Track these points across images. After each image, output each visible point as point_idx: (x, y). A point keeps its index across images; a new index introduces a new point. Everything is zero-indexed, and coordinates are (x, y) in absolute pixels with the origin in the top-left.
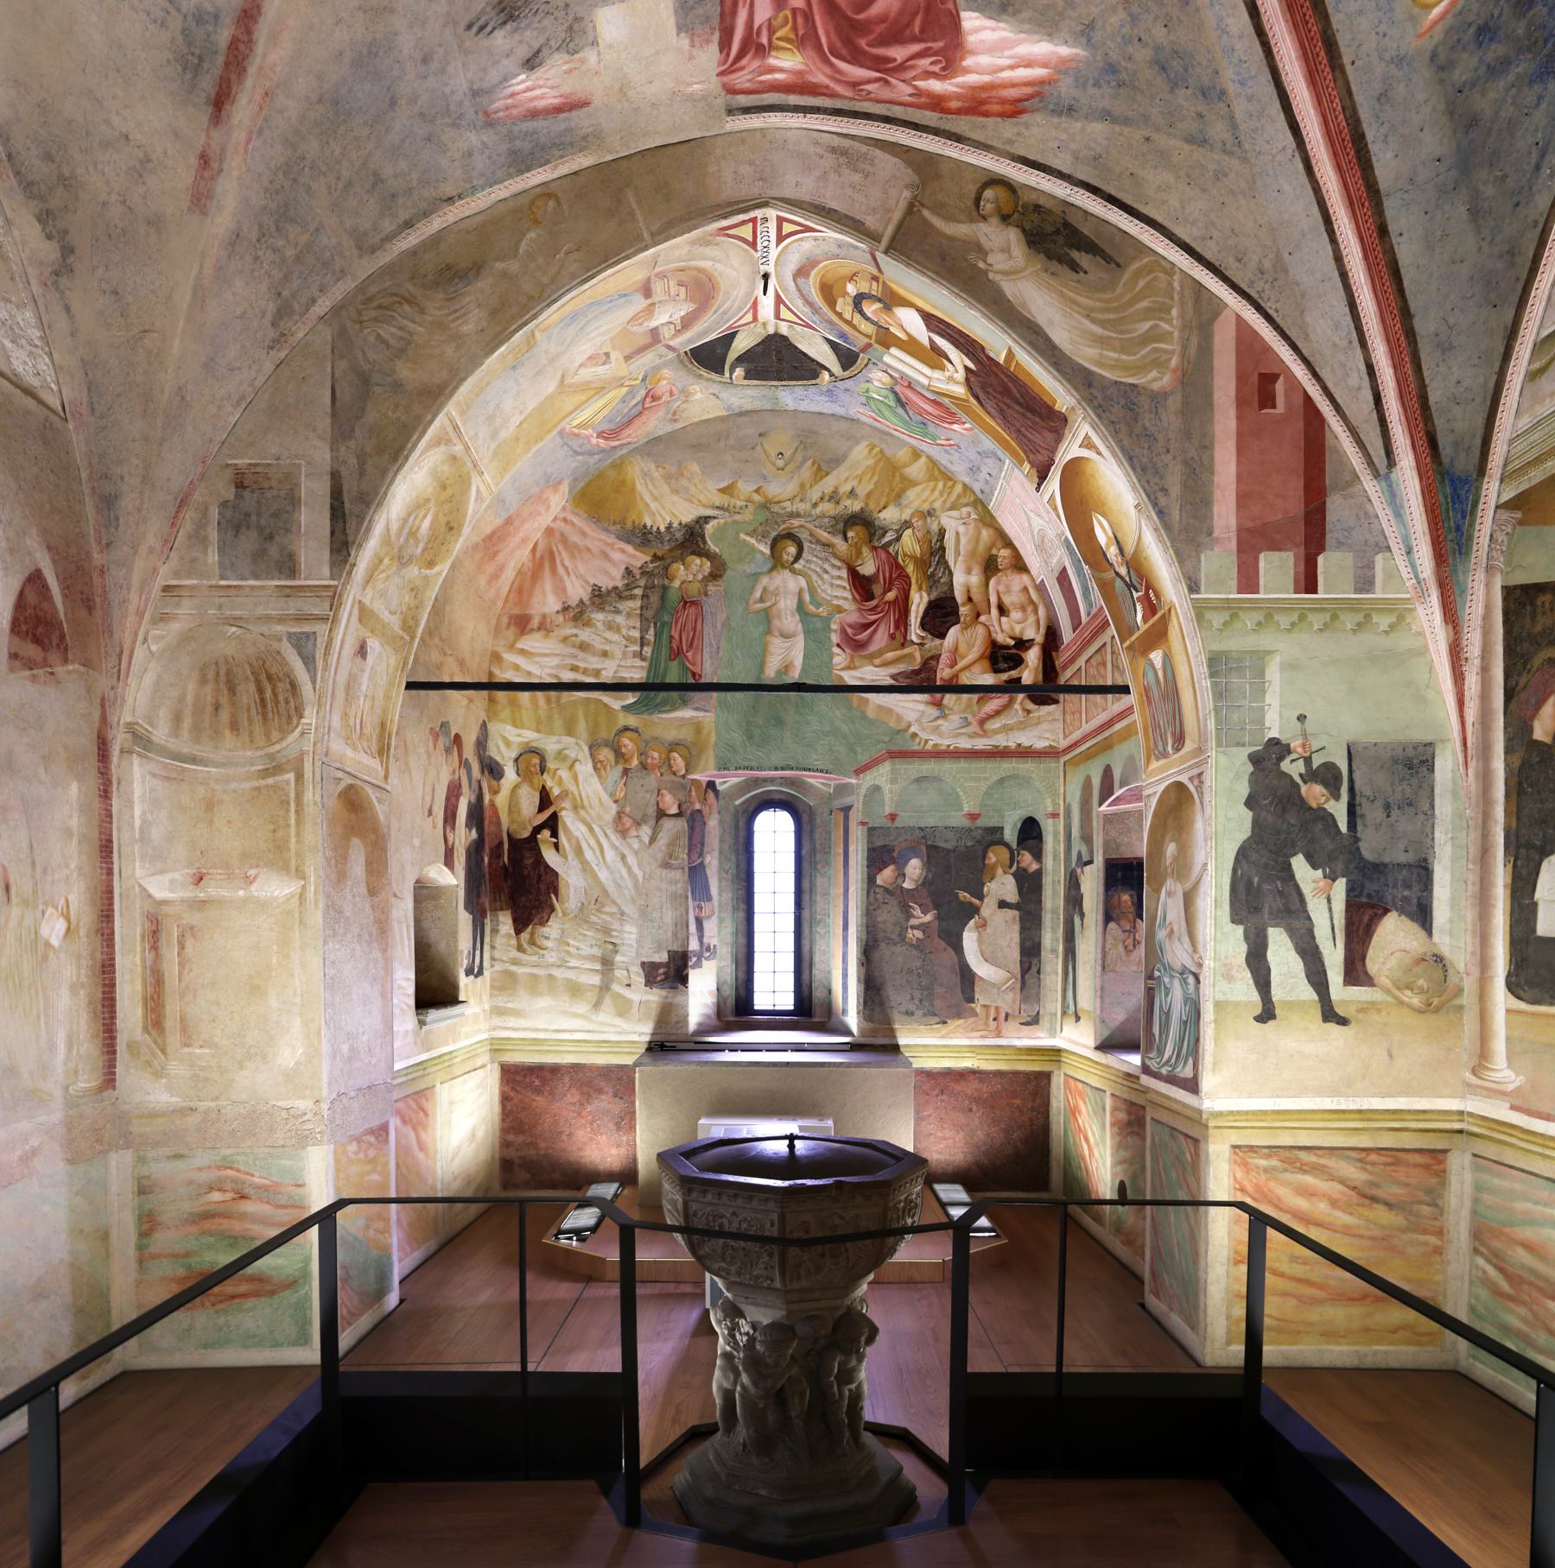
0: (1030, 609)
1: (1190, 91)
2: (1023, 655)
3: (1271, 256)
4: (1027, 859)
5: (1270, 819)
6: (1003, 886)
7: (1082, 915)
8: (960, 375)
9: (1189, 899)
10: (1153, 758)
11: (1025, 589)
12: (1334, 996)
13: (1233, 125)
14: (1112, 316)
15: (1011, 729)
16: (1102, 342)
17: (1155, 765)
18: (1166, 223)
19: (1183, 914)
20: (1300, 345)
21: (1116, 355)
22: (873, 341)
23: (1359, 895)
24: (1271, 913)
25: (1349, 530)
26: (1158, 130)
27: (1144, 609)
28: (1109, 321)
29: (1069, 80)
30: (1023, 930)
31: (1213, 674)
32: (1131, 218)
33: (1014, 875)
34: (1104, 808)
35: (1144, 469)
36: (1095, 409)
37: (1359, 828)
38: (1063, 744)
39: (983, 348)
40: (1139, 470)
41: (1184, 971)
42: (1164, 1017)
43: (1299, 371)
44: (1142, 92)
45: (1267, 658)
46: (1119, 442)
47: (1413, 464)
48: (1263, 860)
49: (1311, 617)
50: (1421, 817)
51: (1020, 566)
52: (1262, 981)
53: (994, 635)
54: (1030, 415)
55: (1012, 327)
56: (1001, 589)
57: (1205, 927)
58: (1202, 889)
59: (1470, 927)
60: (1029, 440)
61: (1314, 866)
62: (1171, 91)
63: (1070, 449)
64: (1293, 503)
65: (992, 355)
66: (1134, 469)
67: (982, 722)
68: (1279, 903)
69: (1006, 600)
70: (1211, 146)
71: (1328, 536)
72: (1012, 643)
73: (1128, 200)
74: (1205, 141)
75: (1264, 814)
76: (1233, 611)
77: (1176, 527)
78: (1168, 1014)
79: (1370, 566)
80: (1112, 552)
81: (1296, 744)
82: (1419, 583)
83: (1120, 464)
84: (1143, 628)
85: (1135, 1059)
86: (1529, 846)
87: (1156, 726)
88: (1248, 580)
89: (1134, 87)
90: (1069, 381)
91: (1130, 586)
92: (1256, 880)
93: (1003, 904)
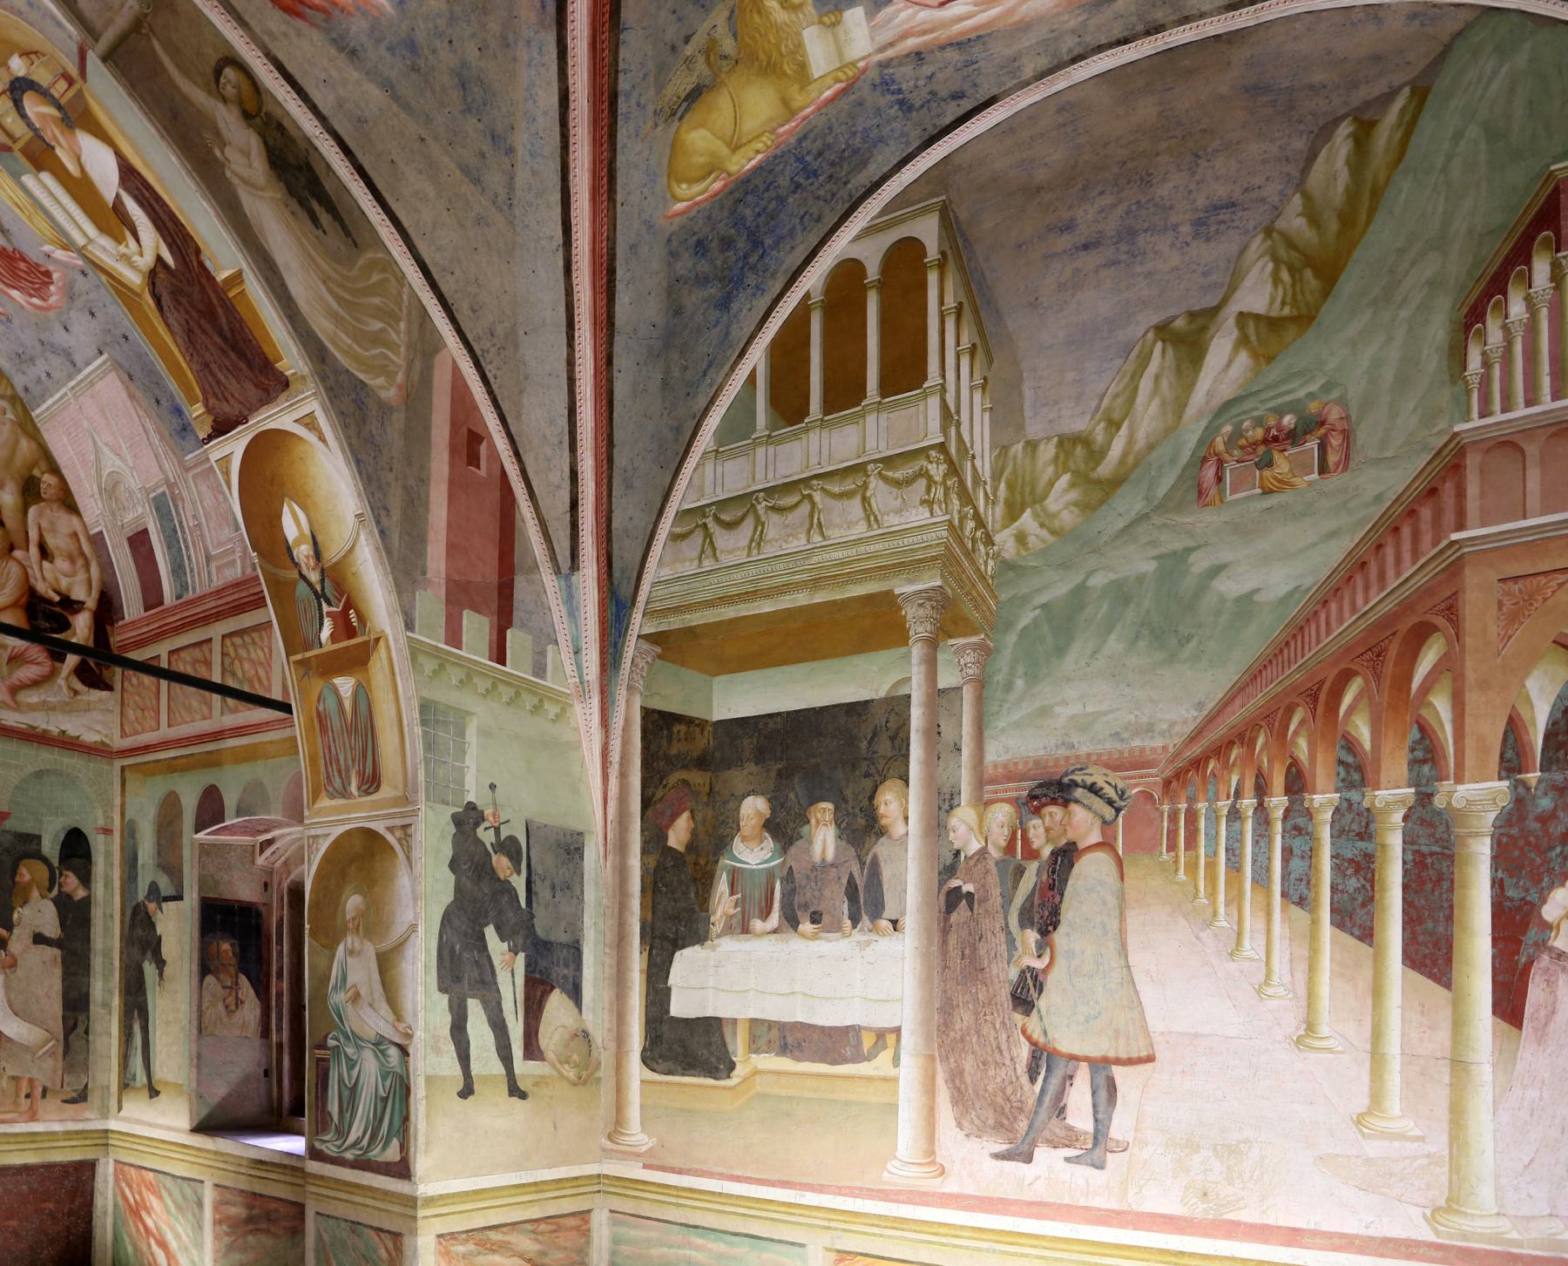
0: (80, 562)
1: (480, 126)
2: (70, 618)
3: (506, 324)
4: (71, 881)
5: (469, 885)
6: (39, 914)
7: (160, 963)
8: (147, 261)
9: (387, 964)
10: (323, 793)
11: (75, 535)
12: (517, 1071)
13: (511, 186)
14: (347, 296)
15: (53, 709)
16: (337, 319)
17: (325, 802)
18: (411, 231)
19: (376, 976)
20: (509, 420)
21: (349, 341)
22: (17, 147)
23: (534, 972)
24: (469, 984)
25: (530, 613)
26: (436, 139)
27: (335, 627)
28: (345, 300)
29: (364, 25)
30: (67, 975)
31: (424, 723)
32: (375, 203)
33: (55, 901)
34: (201, 835)
35: (369, 478)
36: (329, 390)
37: (534, 905)
38: (119, 743)
39: (198, 251)
40: (364, 476)
41: (379, 1043)
42: (346, 1093)
43: (501, 444)
44: (433, 92)
45: (467, 719)
46: (348, 437)
47: (595, 575)
48: (463, 927)
49: (502, 688)
50: (575, 899)
51: (69, 504)
52: (464, 1057)
53: (32, 580)
54: (233, 355)
55: (249, 250)
56: (44, 524)
57: (415, 993)
58: (409, 952)
59: (607, 1006)
60: (218, 382)
61: (503, 941)
62: (463, 112)
63: (279, 417)
64: (487, 571)
65: (208, 264)
66: (360, 474)
67: (14, 690)
68: (476, 974)
69: (51, 542)
70: (483, 189)
71: (515, 613)
72: (57, 598)
73: (380, 186)
74: (479, 180)
75: (464, 879)
76: (443, 661)
77: (396, 554)
78: (354, 1089)
79: (543, 653)
80: (303, 552)
81: (488, 812)
82: (582, 683)
83: (348, 463)
84: (328, 647)
85: (294, 1144)
86: (664, 938)
87: (332, 760)
88: (454, 638)
89: (426, 81)
90: (304, 345)
91: (320, 596)
92: (458, 947)
93: (39, 939)
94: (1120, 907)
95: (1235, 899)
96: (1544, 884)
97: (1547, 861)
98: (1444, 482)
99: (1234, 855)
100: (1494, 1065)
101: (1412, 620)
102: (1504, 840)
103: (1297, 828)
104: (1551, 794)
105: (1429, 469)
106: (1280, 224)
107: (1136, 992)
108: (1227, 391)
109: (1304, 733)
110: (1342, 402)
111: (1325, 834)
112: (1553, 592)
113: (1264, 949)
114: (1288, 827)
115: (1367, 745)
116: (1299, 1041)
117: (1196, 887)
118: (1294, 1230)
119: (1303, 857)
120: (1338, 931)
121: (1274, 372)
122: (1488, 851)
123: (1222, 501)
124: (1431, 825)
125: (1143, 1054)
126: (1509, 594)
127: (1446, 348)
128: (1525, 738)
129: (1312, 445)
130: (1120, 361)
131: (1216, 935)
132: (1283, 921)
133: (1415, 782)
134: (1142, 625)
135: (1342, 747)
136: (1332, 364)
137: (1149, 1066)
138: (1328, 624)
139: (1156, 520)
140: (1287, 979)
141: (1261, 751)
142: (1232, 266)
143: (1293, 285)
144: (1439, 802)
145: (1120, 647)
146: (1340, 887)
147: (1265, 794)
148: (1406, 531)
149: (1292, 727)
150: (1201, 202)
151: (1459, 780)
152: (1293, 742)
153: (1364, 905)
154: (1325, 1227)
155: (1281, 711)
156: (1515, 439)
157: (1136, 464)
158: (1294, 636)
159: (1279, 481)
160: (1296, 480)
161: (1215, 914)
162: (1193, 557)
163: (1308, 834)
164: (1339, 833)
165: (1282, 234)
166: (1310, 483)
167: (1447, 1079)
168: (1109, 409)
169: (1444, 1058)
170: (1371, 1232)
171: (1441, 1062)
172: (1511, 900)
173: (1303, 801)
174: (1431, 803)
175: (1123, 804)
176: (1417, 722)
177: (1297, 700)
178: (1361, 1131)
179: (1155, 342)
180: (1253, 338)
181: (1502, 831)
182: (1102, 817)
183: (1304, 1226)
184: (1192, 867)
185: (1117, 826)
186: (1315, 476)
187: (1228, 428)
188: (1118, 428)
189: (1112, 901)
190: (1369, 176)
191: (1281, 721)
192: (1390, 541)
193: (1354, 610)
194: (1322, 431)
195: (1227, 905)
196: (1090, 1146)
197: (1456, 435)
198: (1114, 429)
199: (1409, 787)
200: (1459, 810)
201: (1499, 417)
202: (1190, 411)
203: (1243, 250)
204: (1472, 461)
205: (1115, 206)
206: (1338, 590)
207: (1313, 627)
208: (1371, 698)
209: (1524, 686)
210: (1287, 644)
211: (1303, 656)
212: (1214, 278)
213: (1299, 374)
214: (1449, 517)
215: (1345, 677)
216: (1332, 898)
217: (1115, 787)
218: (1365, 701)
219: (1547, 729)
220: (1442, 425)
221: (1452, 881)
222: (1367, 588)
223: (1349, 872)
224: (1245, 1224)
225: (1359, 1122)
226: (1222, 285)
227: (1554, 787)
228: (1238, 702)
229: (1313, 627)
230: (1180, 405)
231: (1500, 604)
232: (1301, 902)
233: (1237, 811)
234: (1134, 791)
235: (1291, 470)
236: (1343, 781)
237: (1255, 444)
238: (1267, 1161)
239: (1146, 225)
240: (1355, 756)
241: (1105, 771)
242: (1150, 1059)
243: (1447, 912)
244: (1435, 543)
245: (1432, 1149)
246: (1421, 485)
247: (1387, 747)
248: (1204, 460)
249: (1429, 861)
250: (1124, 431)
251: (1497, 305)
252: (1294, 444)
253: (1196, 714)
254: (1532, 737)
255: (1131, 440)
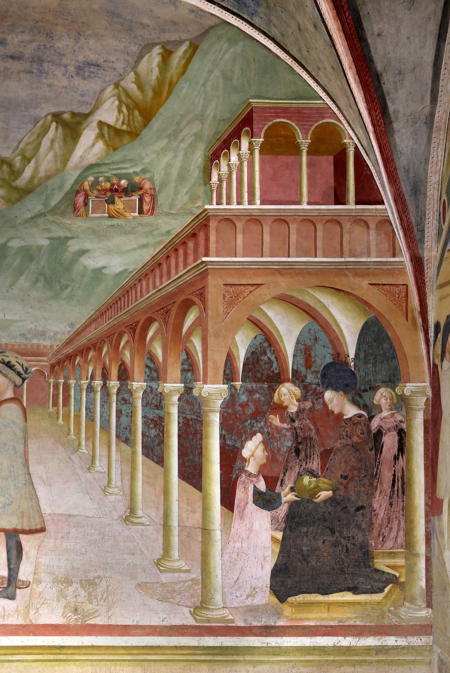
94: (25, 438)
95: (91, 437)
96: (243, 439)
97: (244, 427)
98: (200, 231)
99: (90, 412)
100: (221, 531)
101: (183, 297)
102: (226, 415)
103: (124, 399)
104: (246, 393)
105: (193, 223)
106: (123, 83)
107: (34, 489)
108: (91, 159)
109: (128, 348)
110: (151, 180)
111: (139, 404)
112: (248, 295)
113: (107, 466)
114: (120, 398)
115: (161, 359)
116: (126, 519)
117: (69, 429)
118: (126, 626)
119: (127, 416)
120: (145, 458)
121: (117, 156)
122: (218, 420)
123: (87, 216)
124: (192, 404)
125: (39, 527)
126: (228, 292)
127: (202, 168)
128: (235, 364)
129: (136, 198)
130: (30, 126)
131: (80, 457)
132: (117, 451)
133: (184, 381)
134: (40, 274)
135: (148, 358)
136: (147, 160)
137: (42, 534)
138: (141, 291)
139: (50, 217)
140: (119, 484)
141: (105, 355)
142: (97, 96)
143: (129, 116)
144: (195, 392)
145: (27, 284)
146: (147, 434)
147: (107, 379)
148: (181, 252)
149: (122, 344)
150: (81, 58)
151: (205, 382)
152: (122, 352)
153: (159, 444)
154: (141, 623)
155: (116, 335)
156: (233, 218)
157: (39, 185)
158: (124, 295)
159: (118, 212)
160: (127, 214)
161: (80, 445)
162: (70, 242)
163: (130, 403)
164: (146, 405)
165: (124, 89)
166: (134, 217)
167: (200, 539)
168: (23, 150)
169: (199, 528)
170: (165, 623)
171: (197, 530)
172: (229, 446)
173: (127, 385)
174: (191, 393)
175: (27, 376)
176: (185, 350)
177: (125, 330)
178: (159, 569)
179: (51, 122)
180: (106, 136)
181: (225, 410)
182: (14, 383)
183: (131, 624)
184: (67, 417)
185: (23, 389)
186: (137, 214)
187: (91, 179)
188: (29, 162)
189: (20, 434)
190: (169, 75)
191: (116, 340)
192: (173, 255)
193: (155, 287)
194: (141, 192)
195: (86, 440)
196: (5, 586)
197: (205, 210)
198: (26, 162)
199: (181, 383)
200: (205, 398)
201: (224, 206)
202: (70, 164)
203: (103, 90)
204: (213, 225)
205: (30, 42)
206: (147, 275)
207: (134, 292)
208: (162, 334)
209: (234, 338)
210: (120, 298)
211: (128, 307)
212: (86, 99)
213: (130, 161)
214: (202, 249)
215: (150, 321)
216: (142, 440)
217: (22, 366)
218: (160, 335)
219: (244, 361)
220: (199, 204)
221: (202, 435)
222: (161, 277)
223: (151, 426)
224: (99, 626)
225: (158, 564)
226: (90, 104)
227: (247, 390)
228: (93, 326)
229: (134, 292)
230: (66, 159)
231: (224, 297)
232: (127, 441)
233: (92, 387)
234: (33, 369)
235: (124, 208)
236: (148, 376)
237: (105, 190)
238: (110, 588)
239: (49, 59)
240: (154, 364)
241: (16, 355)
242: (43, 530)
243: (200, 450)
244: (195, 261)
245: (193, 576)
246: (189, 231)
247: (170, 361)
248: (78, 192)
249: (191, 423)
250: (32, 164)
251: (225, 154)
252: (126, 195)
253: (69, 329)
254: (238, 364)
255: (36, 170)
